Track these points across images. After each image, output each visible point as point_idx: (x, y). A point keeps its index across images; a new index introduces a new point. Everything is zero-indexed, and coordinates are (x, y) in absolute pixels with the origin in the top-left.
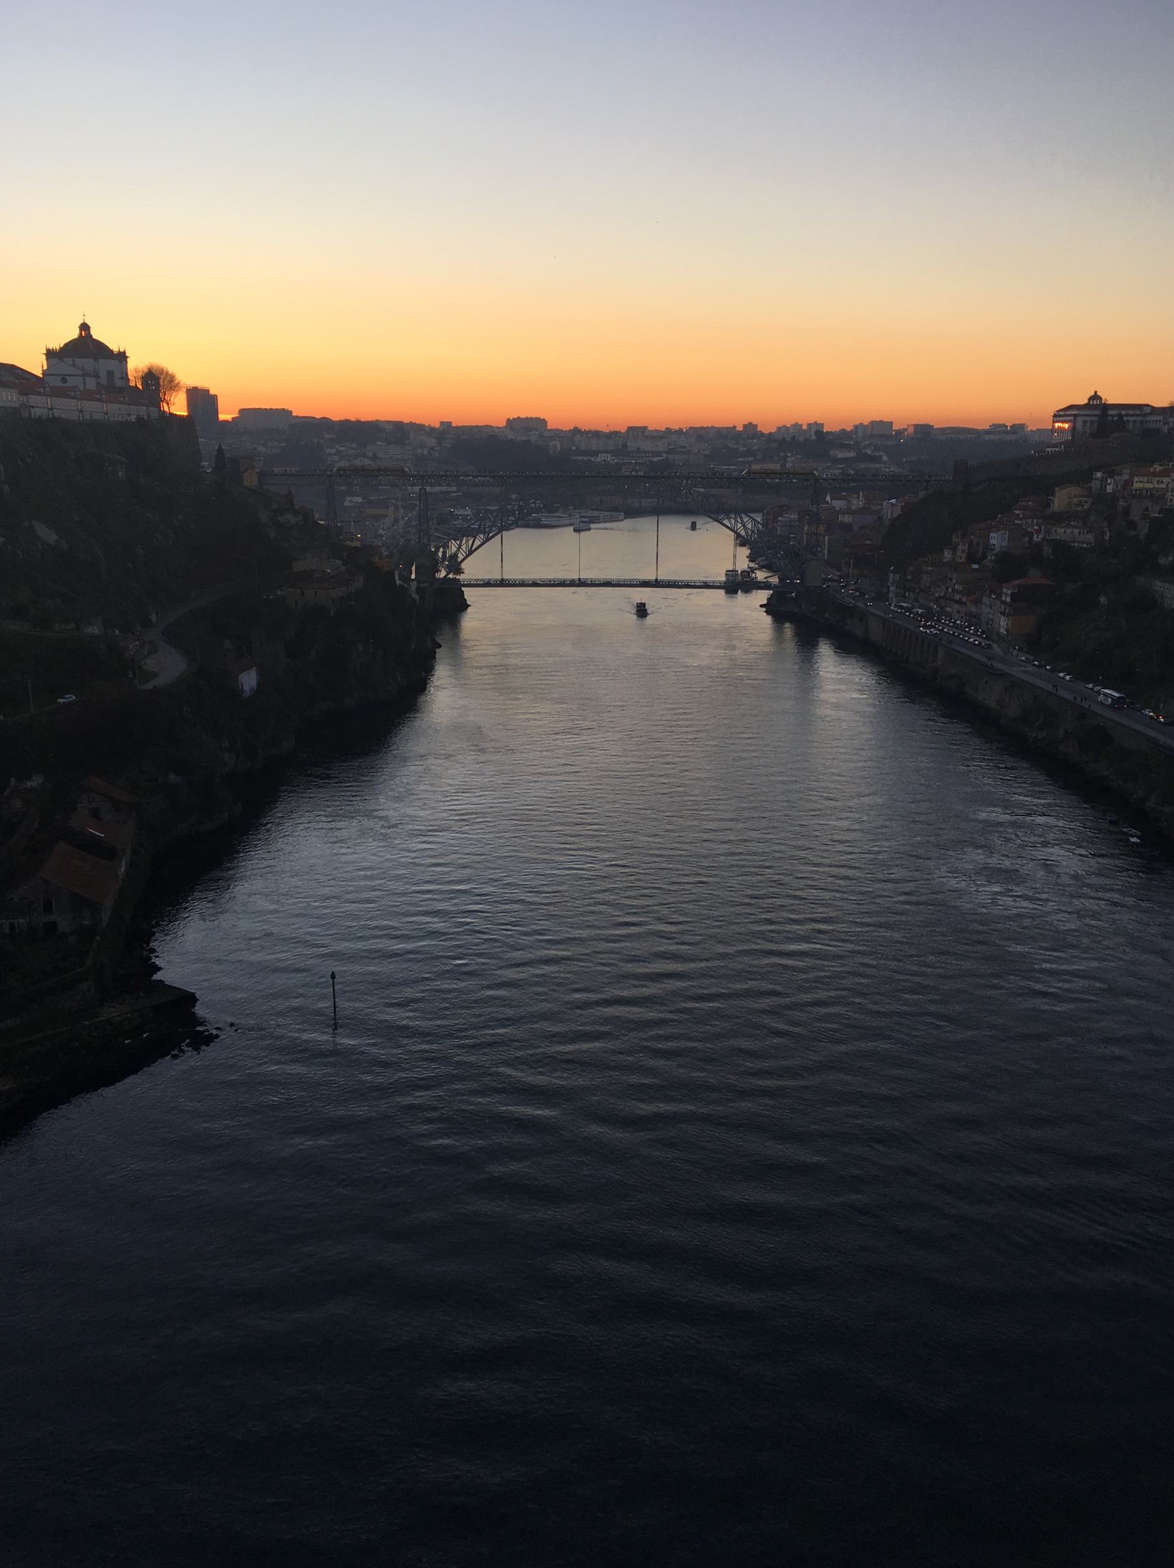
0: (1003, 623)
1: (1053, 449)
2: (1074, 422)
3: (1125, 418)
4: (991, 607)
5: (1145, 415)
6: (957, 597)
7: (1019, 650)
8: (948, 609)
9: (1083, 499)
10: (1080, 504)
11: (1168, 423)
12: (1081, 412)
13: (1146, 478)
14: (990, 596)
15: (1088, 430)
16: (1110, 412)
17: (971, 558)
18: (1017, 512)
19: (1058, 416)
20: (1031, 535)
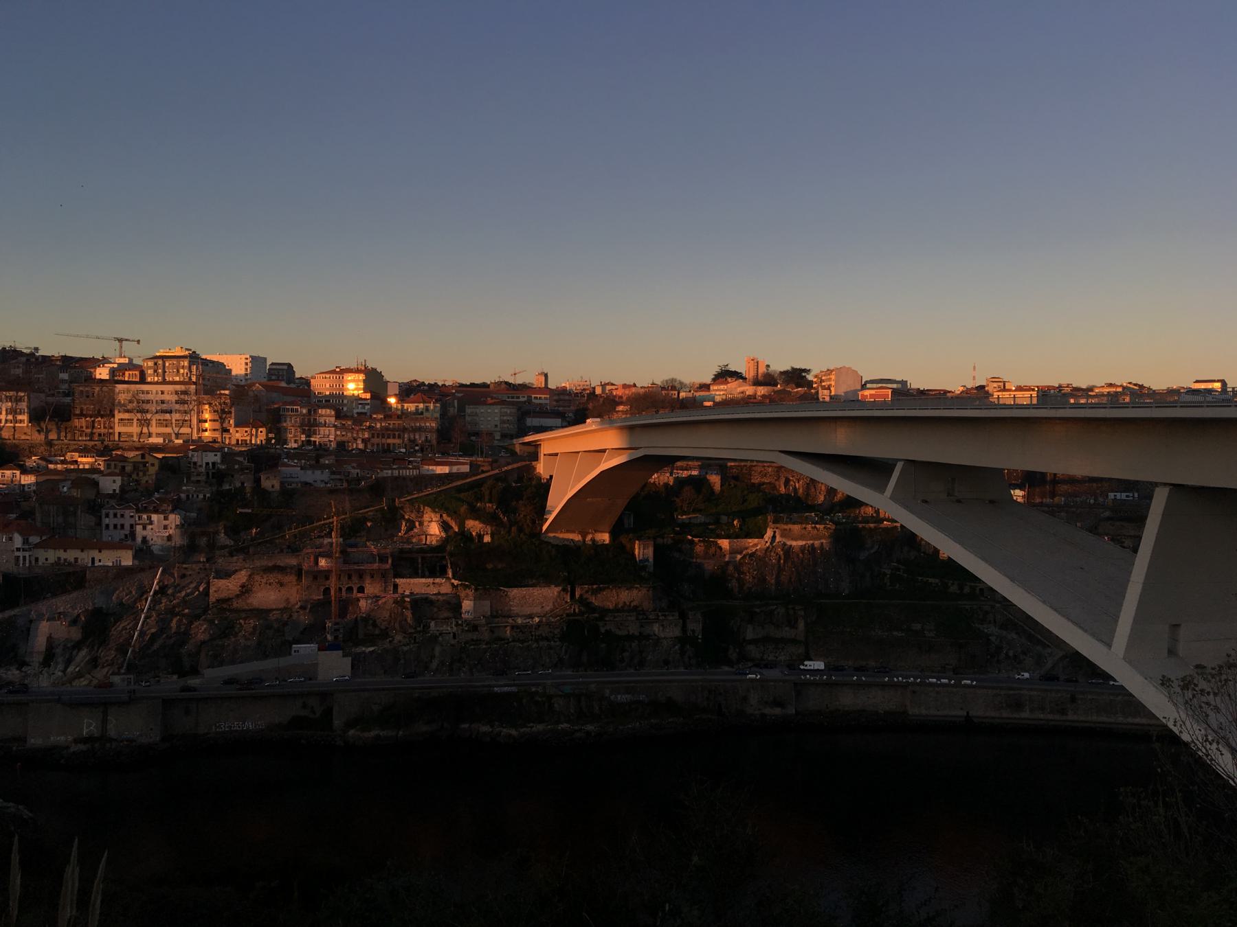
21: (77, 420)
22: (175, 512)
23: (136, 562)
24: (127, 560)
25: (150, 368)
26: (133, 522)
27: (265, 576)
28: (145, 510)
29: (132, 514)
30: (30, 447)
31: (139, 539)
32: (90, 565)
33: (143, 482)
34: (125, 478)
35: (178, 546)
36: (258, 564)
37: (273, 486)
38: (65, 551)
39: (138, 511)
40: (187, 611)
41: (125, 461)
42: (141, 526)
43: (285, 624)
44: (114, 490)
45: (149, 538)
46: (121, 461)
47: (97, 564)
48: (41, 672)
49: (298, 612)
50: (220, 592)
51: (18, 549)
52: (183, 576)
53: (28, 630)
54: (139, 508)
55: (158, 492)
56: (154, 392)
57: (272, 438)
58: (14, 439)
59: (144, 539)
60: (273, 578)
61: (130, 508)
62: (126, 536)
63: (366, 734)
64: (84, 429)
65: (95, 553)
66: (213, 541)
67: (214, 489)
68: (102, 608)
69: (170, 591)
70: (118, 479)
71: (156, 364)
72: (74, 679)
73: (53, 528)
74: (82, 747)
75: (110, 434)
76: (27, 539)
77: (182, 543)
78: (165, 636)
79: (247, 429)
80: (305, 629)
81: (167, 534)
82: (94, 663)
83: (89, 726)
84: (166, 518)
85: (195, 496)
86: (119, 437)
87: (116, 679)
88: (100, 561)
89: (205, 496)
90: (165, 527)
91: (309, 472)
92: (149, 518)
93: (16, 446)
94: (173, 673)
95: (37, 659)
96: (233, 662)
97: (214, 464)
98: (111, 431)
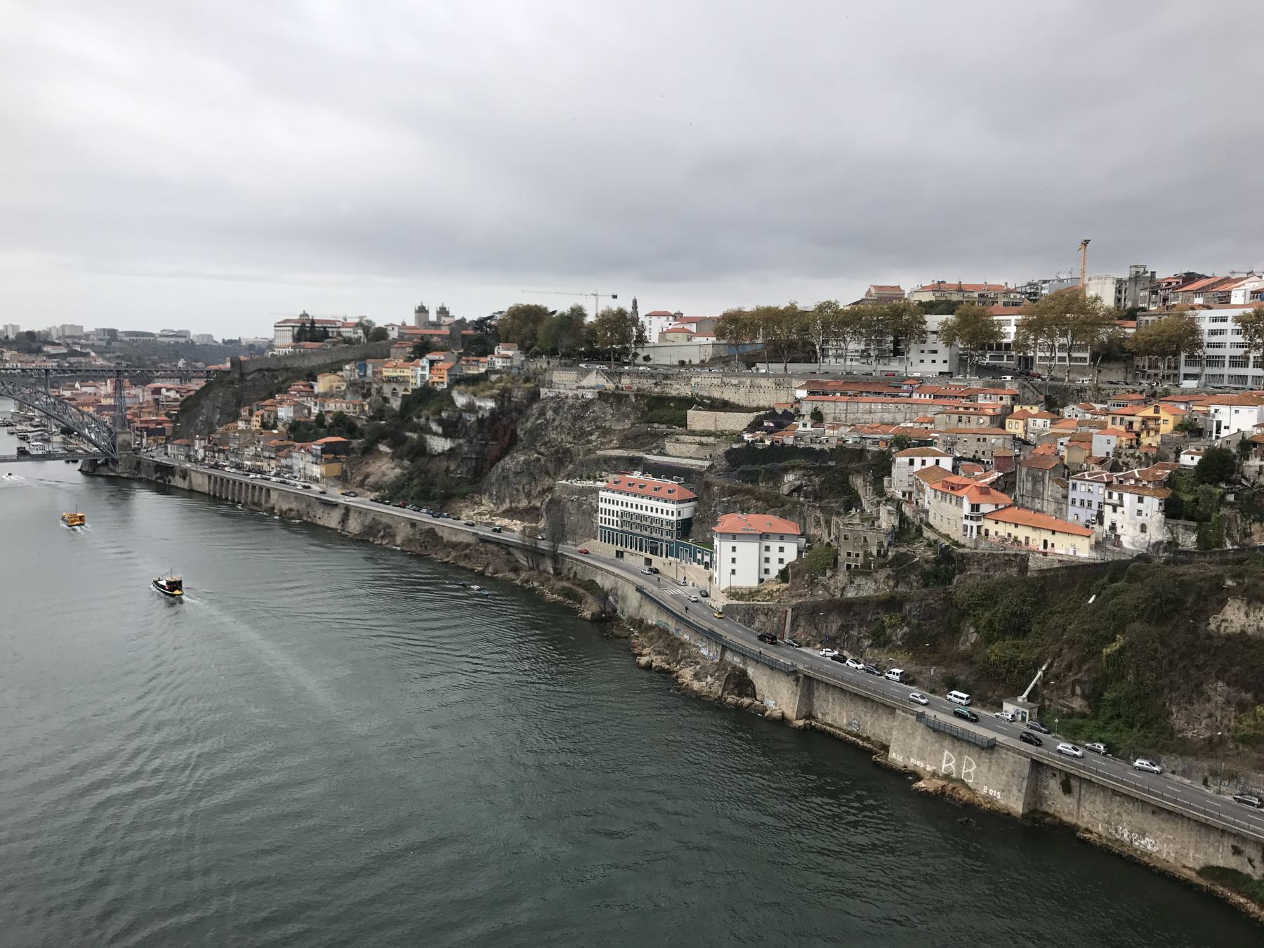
1: (284, 350)
5: (339, 327)
6: (267, 454)
10: (338, 387)
11: (356, 333)
13: (391, 370)
16: (316, 325)
17: (264, 425)
18: (292, 393)
20: (309, 409)
23: (1094, 555)
26: (1102, 501)
31: (1107, 524)
32: (1041, 548)
35: (1153, 541)
45: (1118, 525)
51: (966, 517)
54: (1111, 482)
59: (1113, 527)
64: (1146, 369)
65: (1047, 536)
73: (1022, 495)
75: (1175, 375)
88: (1053, 545)
92: (1121, 497)
98: (1176, 372)
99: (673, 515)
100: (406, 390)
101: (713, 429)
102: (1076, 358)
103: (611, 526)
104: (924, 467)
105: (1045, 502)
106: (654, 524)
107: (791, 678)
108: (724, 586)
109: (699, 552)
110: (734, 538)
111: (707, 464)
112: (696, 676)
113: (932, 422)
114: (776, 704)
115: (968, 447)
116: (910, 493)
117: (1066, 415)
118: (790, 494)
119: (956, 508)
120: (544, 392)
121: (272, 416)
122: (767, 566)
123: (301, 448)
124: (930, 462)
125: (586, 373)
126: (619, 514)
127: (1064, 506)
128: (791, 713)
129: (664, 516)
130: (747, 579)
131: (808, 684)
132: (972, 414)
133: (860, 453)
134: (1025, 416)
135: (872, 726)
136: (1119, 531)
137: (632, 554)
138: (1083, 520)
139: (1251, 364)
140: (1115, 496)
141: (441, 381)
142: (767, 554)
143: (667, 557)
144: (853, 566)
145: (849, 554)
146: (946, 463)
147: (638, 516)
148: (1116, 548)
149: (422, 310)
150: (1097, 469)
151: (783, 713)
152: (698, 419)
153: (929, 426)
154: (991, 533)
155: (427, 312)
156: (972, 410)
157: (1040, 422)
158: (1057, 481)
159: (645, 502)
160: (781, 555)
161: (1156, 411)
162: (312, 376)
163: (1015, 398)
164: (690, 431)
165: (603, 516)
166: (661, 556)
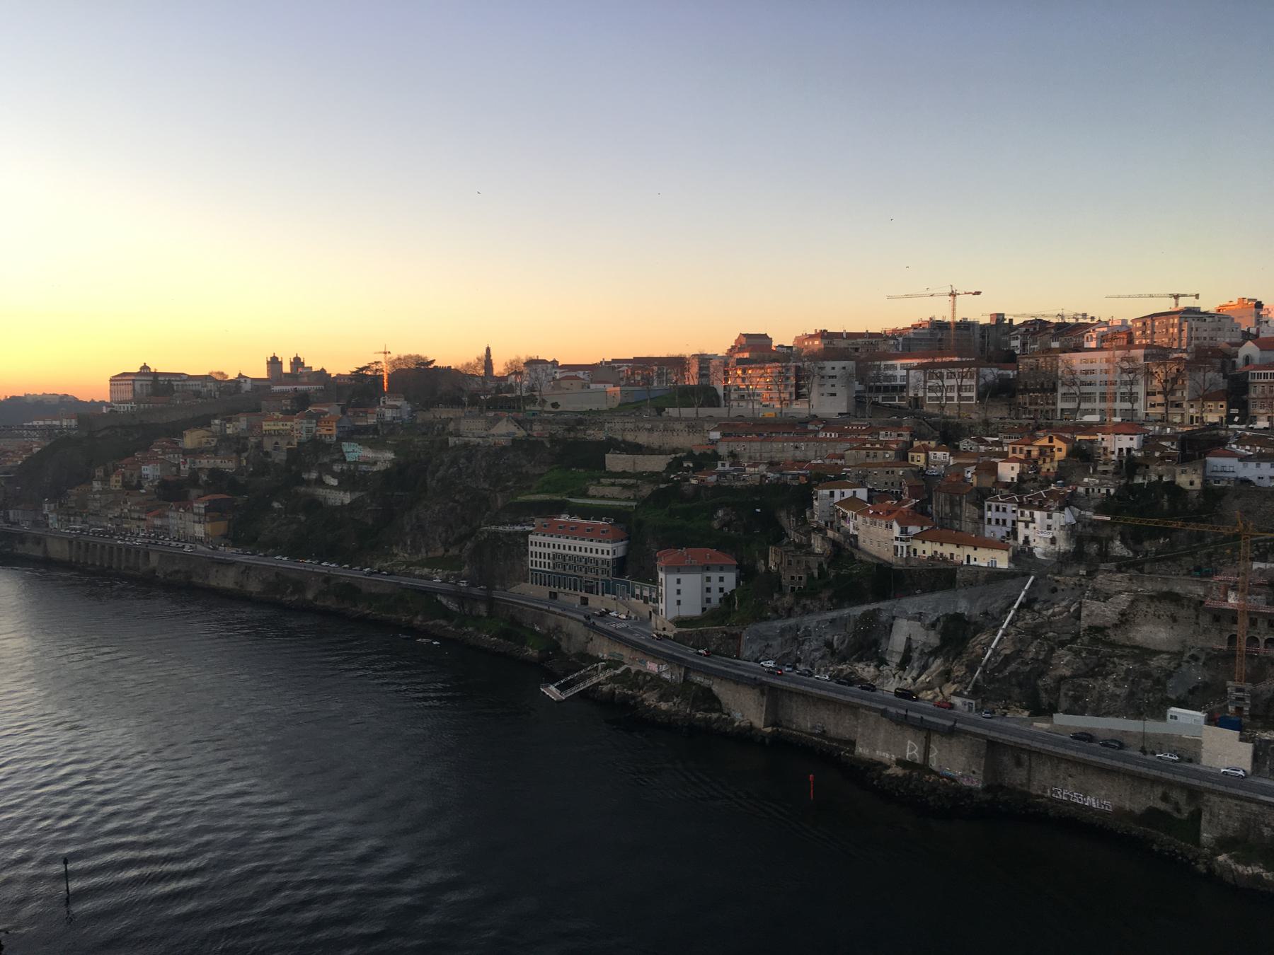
0: (199, 530)
2: (134, 387)
3: (175, 383)
4: (181, 518)
5: (184, 380)
6: (136, 515)
7: (225, 546)
8: (124, 526)
9: (210, 439)
10: (208, 442)
11: (206, 386)
12: (138, 378)
13: (272, 423)
14: (177, 510)
15: (145, 391)
16: (160, 378)
17: (126, 485)
18: (156, 450)
19: (114, 380)
21: (1021, 396)
22: (1067, 511)
23: (1012, 566)
24: (1002, 561)
25: (1138, 329)
26: (1015, 519)
27: (1153, 606)
28: (1030, 505)
29: (1014, 509)
30: (970, 427)
31: (1021, 539)
32: (965, 563)
33: (1044, 470)
34: (1026, 465)
36: (1149, 587)
37: (1192, 483)
38: (941, 545)
39: (1021, 505)
40: (1051, 634)
41: (1031, 445)
42: (1023, 524)
43: (1169, 675)
44: (1012, 479)
45: (1031, 539)
46: (1027, 445)
47: (972, 562)
48: (894, 677)
49: (1188, 662)
50: (1093, 617)
51: (897, 539)
52: (1054, 590)
53: (891, 625)
55: (1055, 482)
56: (1098, 361)
57: (1236, 415)
58: (959, 417)
59: (1026, 541)
60: (1166, 608)
61: (1012, 501)
62: (1008, 532)
63: (1240, 868)
64: (1028, 406)
65: (969, 551)
66: (1106, 550)
67: (1123, 482)
68: (964, 614)
69: (1037, 607)
70: (1017, 466)
71: (1144, 324)
72: (923, 689)
73: (941, 518)
74: (899, 771)
75: (1053, 410)
76: (906, 528)
77: (1067, 548)
78: (1020, 660)
79: (1221, 403)
80: (1196, 688)
81: (1051, 536)
82: (946, 676)
83: (912, 750)
84: (1050, 517)
85: (1096, 490)
86: (1061, 413)
87: (957, 701)
88: (975, 560)
89: (1108, 491)
90: (1049, 528)
91: (1252, 465)
92: (1032, 515)
93: (958, 425)
94: (1026, 708)
95: (897, 659)
96: (1096, 713)
97: (1129, 450)
98: (1053, 407)
99: (608, 554)
100: (289, 443)
101: (627, 469)
102: (963, 397)
103: (542, 569)
104: (843, 498)
105: (963, 524)
106: (589, 564)
107: (757, 691)
108: (670, 617)
109: (637, 588)
110: (679, 571)
111: (634, 504)
112: (662, 698)
113: (842, 457)
114: (743, 716)
115: (879, 479)
116: (832, 523)
117: (961, 447)
118: (721, 529)
119: (886, 532)
120: (452, 441)
121: (135, 476)
122: (709, 595)
123: (180, 507)
124: (848, 493)
125: (496, 420)
126: (551, 556)
127: (981, 526)
128: (759, 723)
129: (600, 555)
130: (692, 608)
131: (773, 695)
132: (878, 449)
133: (779, 488)
134: (926, 450)
135: (837, 725)
136: (1032, 544)
137: (567, 594)
138: (998, 536)
139: (1118, 399)
140: (1027, 512)
141: (328, 432)
142: (708, 585)
143: (603, 595)
144: (797, 589)
145: (793, 578)
146: (862, 494)
147: (572, 557)
148: (1028, 559)
149: (274, 363)
150: (1006, 492)
151: (751, 723)
152: (615, 462)
153: (839, 462)
154: (919, 553)
155: (281, 363)
156: (878, 446)
157: (939, 454)
158: (974, 504)
159: (578, 543)
160: (721, 585)
161: (1051, 440)
162: (175, 431)
163: (914, 435)
164: (607, 472)
165: (534, 559)
166: (597, 594)
